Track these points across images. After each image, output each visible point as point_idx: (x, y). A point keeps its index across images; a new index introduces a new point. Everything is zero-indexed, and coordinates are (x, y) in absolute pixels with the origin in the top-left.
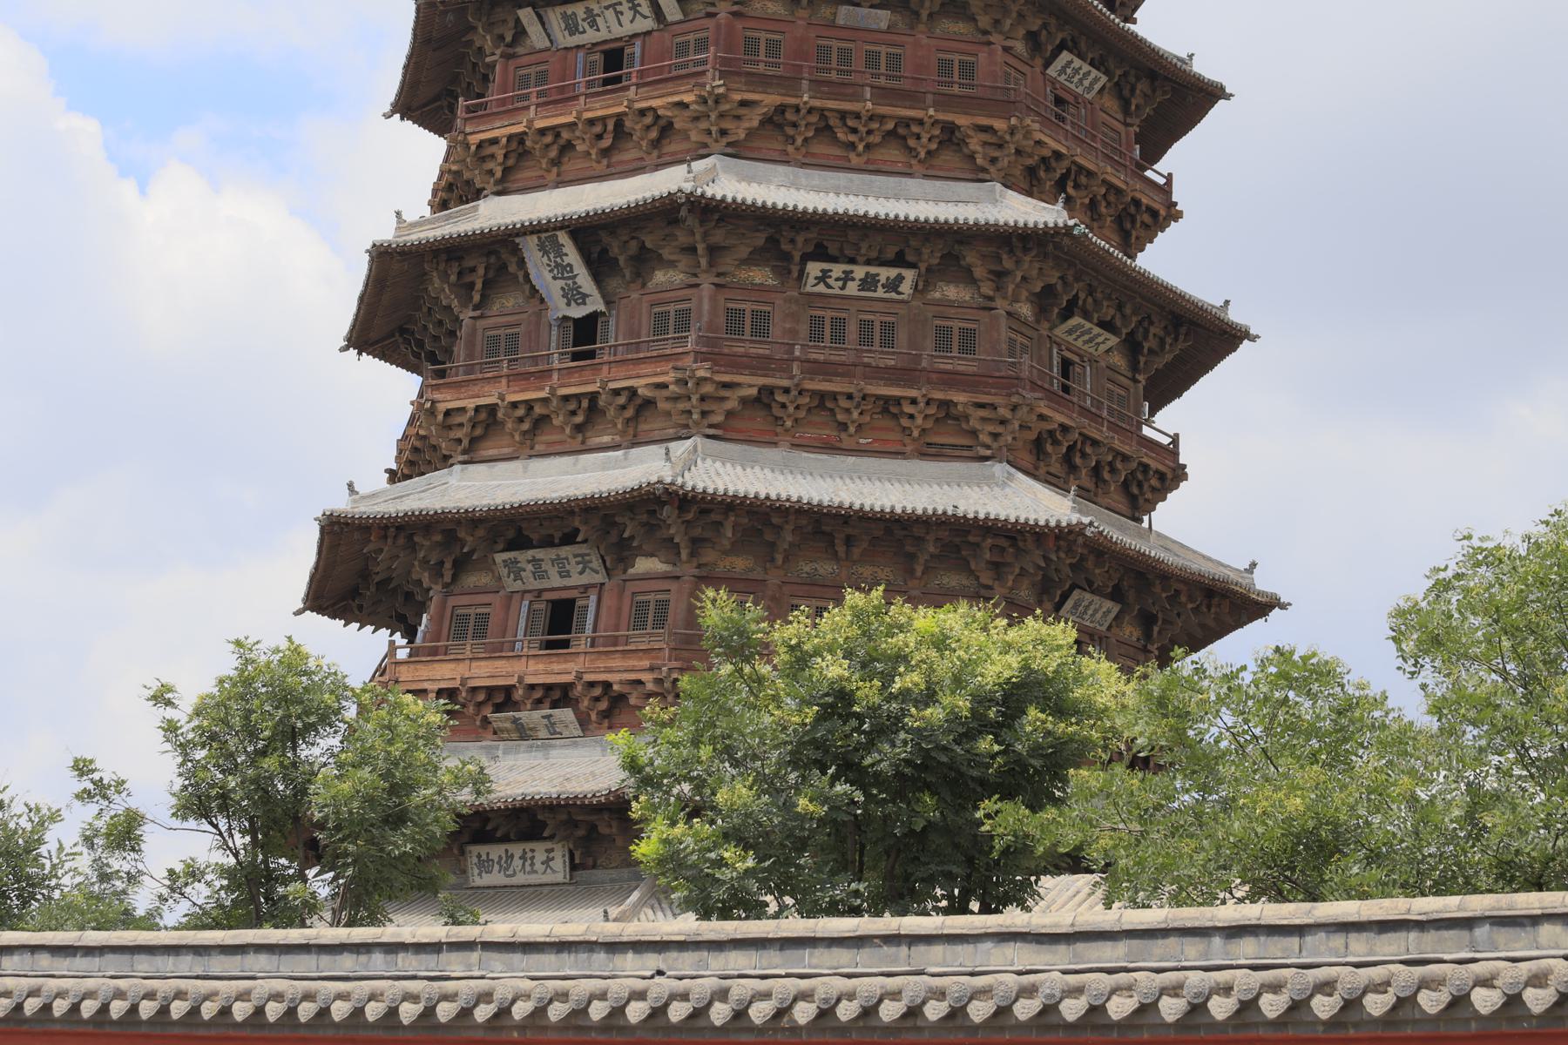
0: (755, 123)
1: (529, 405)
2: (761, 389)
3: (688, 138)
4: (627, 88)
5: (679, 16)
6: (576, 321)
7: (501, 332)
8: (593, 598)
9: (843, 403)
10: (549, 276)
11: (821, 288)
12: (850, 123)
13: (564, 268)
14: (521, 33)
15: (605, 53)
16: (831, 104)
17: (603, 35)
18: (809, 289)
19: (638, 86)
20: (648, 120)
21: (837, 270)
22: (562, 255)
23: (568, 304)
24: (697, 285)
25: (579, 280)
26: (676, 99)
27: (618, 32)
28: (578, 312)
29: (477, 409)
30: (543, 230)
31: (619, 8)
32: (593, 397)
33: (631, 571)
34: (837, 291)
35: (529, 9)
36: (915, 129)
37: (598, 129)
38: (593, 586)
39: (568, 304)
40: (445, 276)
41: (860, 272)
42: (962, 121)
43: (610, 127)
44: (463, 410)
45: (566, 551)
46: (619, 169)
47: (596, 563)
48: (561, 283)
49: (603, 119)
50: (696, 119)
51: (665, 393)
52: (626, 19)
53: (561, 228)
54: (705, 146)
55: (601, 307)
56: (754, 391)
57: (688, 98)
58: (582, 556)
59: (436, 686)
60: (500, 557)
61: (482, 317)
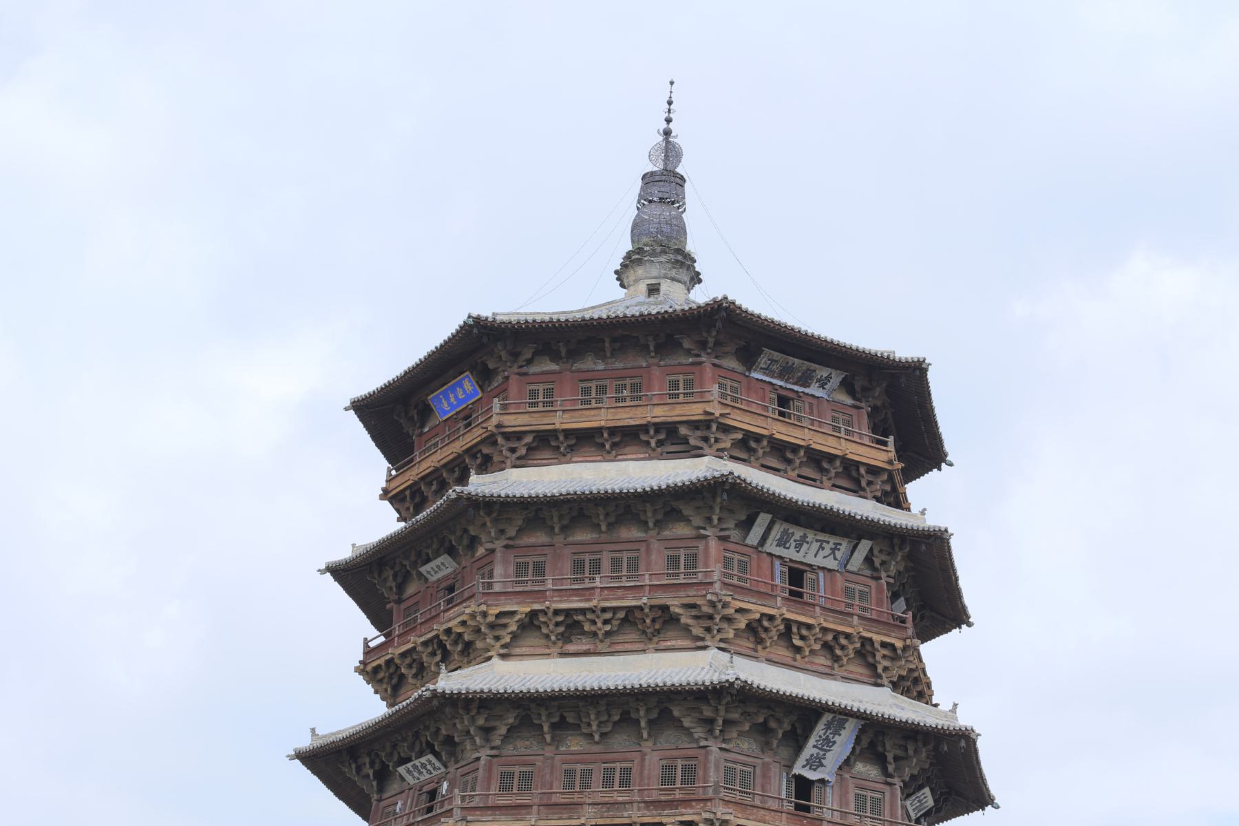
3: (876, 668)
4: (851, 615)
7: (739, 767)
14: (747, 525)
15: (791, 569)
19: (861, 618)
22: (837, 733)
24: (890, 784)
25: (829, 755)
27: (810, 559)
28: (812, 775)
30: (843, 714)
31: (825, 545)
40: (727, 711)
46: (814, 668)
48: (815, 751)
49: (825, 630)
50: (884, 657)
53: (863, 719)
54: (880, 677)
57: (899, 644)
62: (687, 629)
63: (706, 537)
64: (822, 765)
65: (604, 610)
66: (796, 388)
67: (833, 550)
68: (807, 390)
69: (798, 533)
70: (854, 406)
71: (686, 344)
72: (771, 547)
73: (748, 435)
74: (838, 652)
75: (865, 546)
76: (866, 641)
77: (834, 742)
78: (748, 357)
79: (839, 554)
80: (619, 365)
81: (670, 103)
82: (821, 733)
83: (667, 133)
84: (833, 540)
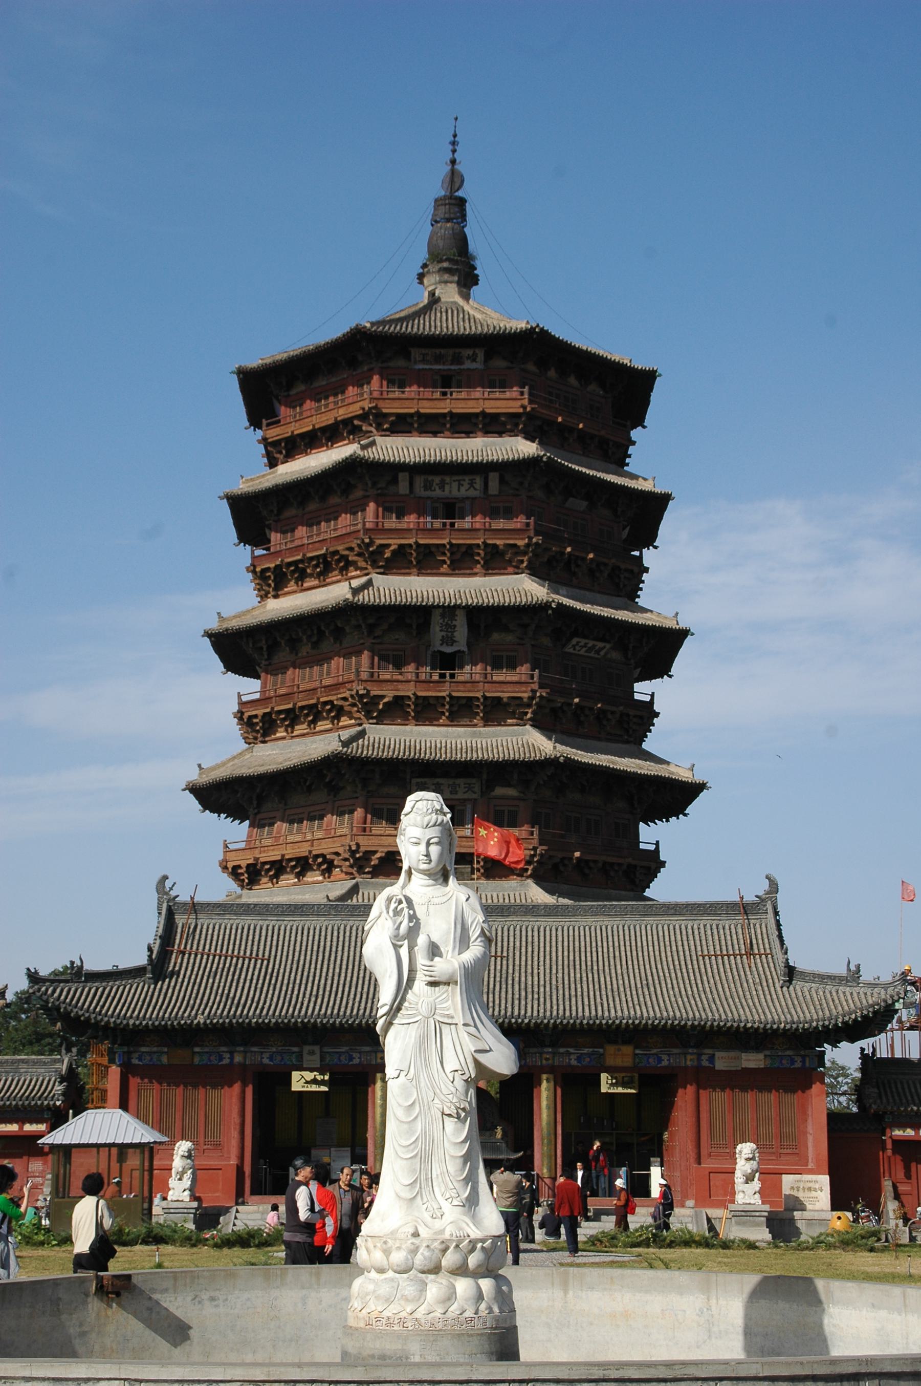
0: (546, 560)
1: (425, 698)
2: (563, 703)
5: (496, 493)
6: (442, 654)
8: (469, 807)
9: (587, 712)
10: (438, 629)
11: (571, 651)
12: (579, 562)
13: (450, 626)
16: (577, 554)
17: (446, 493)
18: (567, 650)
20: (489, 550)
21: (583, 641)
23: (441, 645)
25: (455, 634)
26: (512, 542)
28: (448, 650)
29: (396, 698)
32: (470, 699)
33: (493, 794)
34: (576, 652)
35: (407, 474)
36: (602, 568)
37: (455, 550)
38: (469, 800)
39: (441, 645)
41: (591, 643)
42: (623, 566)
43: (463, 549)
44: (383, 697)
45: (461, 781)
47: (477, 788)
48: (444, 633)
49: (459, 545)
50: (516, 554)
51: (518, 702)
52: (463, 489)
55: (465, 649)
56: (559, 705)
57: (521, 543)
58: (469, 784)
59: (386, 850)
60: (414, 781)
61: (380, 643)
62: (354, 564)
63: (368, 496)
64: (455, 641)
65: (312, 558)
66: (453, 367)
67: (471, 484)
68: (462, 367)
69: (437, 479)
70: (509, 368)
71: (360, 358)
72: (420, 491)
73: (400, 416)
74: (477, 558)
75: (494, 477)
76: (495, 546)
77: (455, 626)
78: (407, 356)
79: (477, 486)
80: (334, 380)
81: (455, 136)
82: (441, 621)
83: (453, 162)
84: (467, 478)
